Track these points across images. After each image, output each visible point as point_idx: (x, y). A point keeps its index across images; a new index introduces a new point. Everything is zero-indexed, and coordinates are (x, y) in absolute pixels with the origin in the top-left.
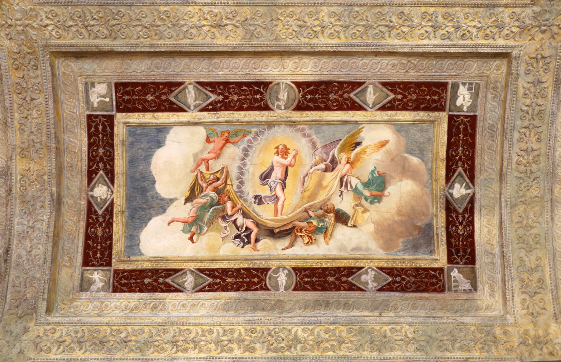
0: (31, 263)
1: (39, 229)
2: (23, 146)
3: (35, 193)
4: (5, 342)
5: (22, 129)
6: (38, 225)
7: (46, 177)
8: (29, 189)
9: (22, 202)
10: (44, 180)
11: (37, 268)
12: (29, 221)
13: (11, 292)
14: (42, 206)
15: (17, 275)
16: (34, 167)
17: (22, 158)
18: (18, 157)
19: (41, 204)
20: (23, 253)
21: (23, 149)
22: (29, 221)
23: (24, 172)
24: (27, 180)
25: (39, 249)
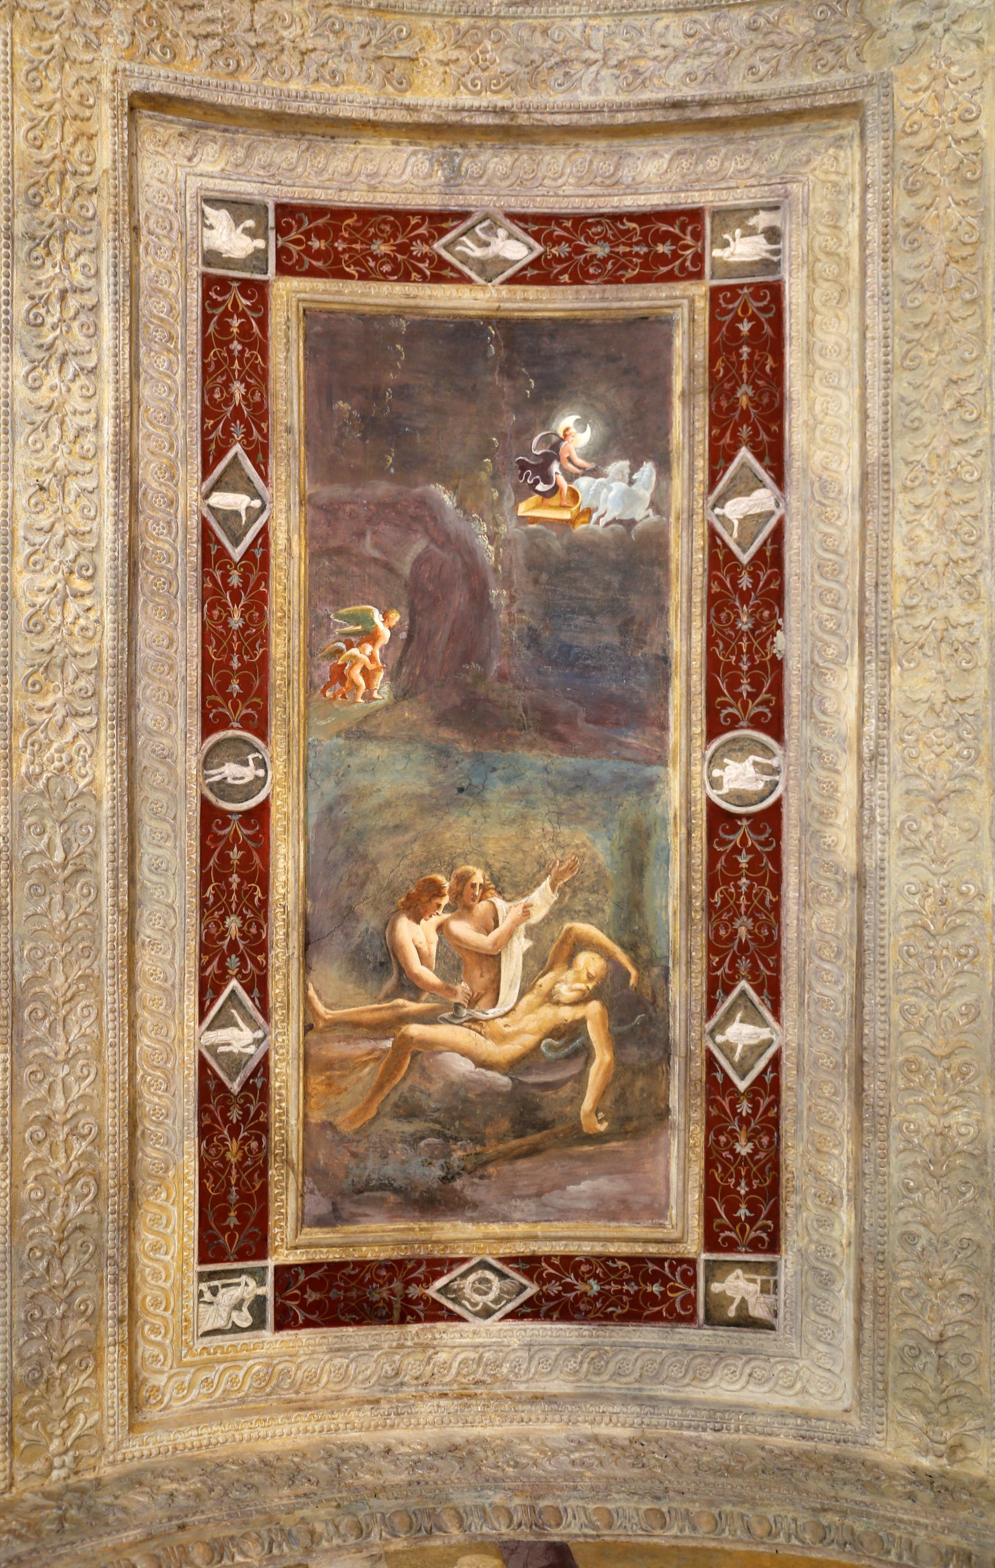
0: (708, 44)
1: (610, 35)
2: (378, 78)
3: (509, 54)
4: (947, 36)
5: (333, 74)
6: (598, 40)
7: (463, 23)
8: (495, 70)
9: (534, 86)
10: (473, 27)
11: (722, 24)
12: (588, 63)
13: (795, 75)
14: (545, 32)
15: (744, 67)
16: (435, 51)
17: (410, 84)
18: (408, 94)
19: (537, 34)
20: (678, 69)
21: (387, 78)
22: (588, 63)
23: (451, 81)
24: (472, 75)
25: (667, 27)
